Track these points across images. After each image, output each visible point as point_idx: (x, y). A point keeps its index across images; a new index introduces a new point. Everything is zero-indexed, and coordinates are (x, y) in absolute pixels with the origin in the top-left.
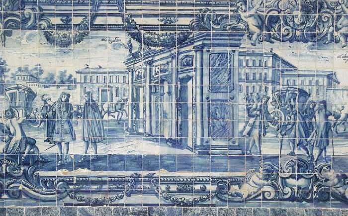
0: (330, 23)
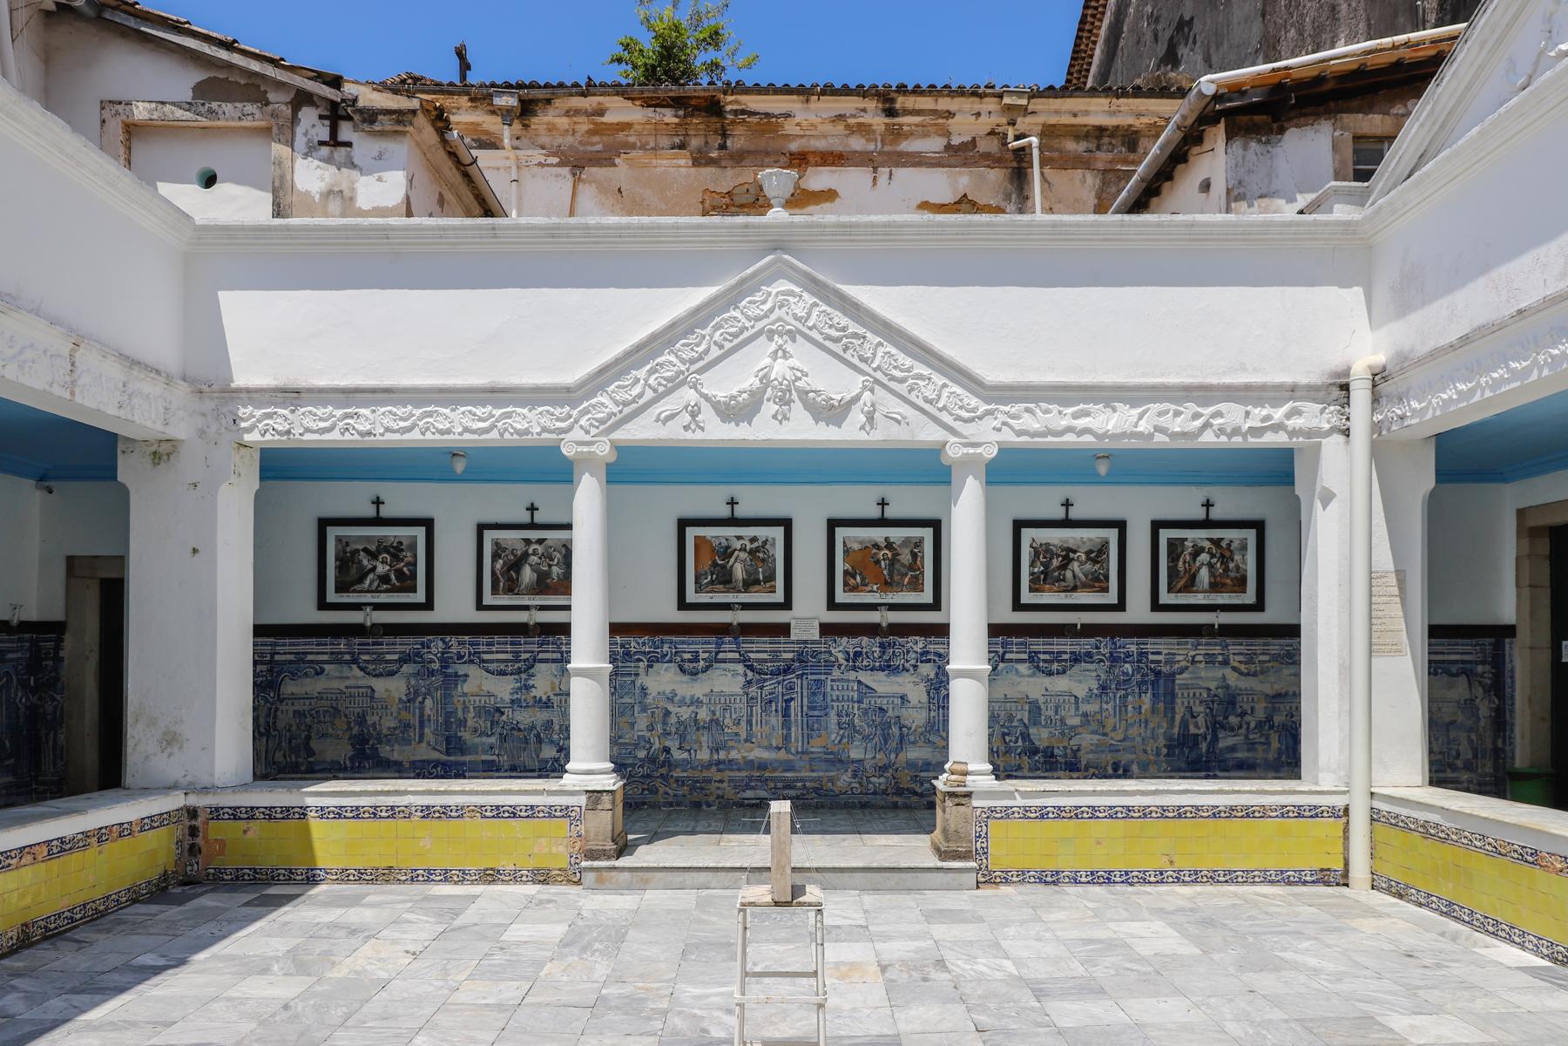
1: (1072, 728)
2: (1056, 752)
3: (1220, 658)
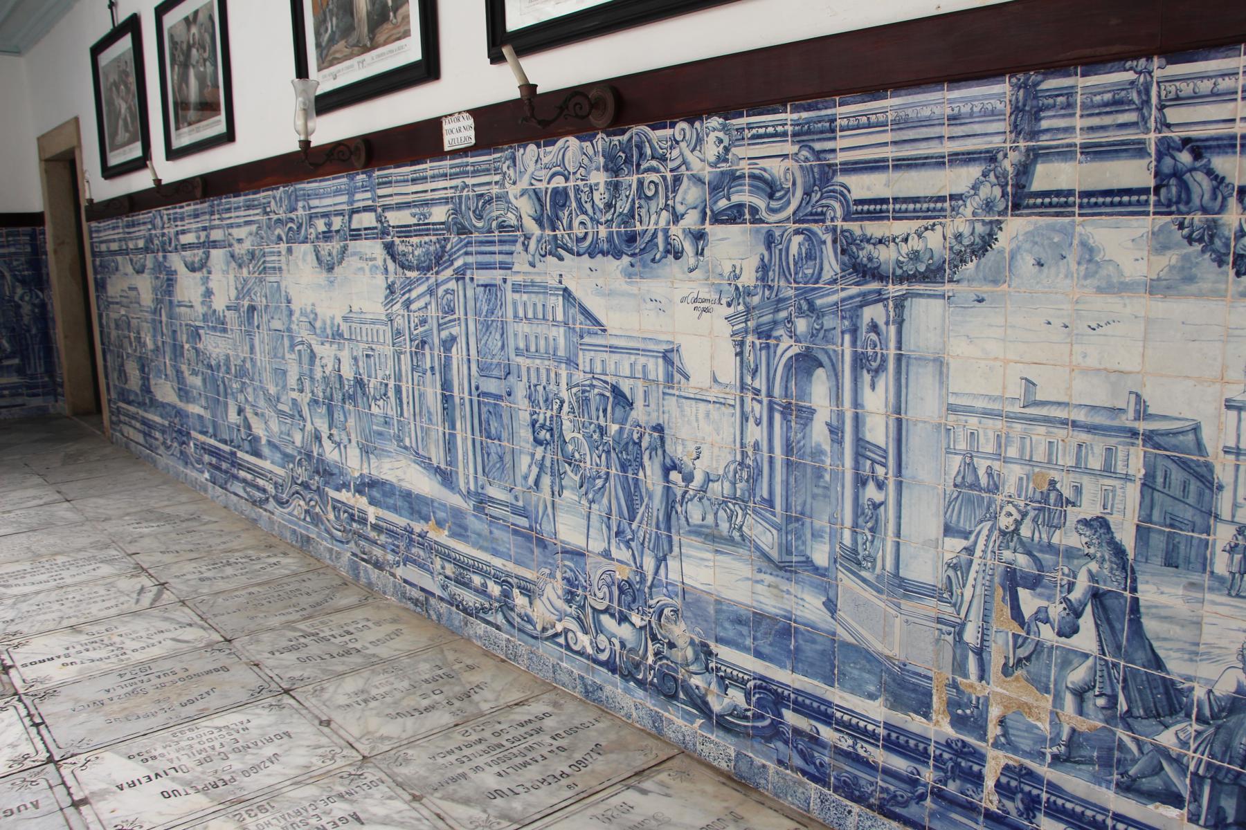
0: (662, 202)
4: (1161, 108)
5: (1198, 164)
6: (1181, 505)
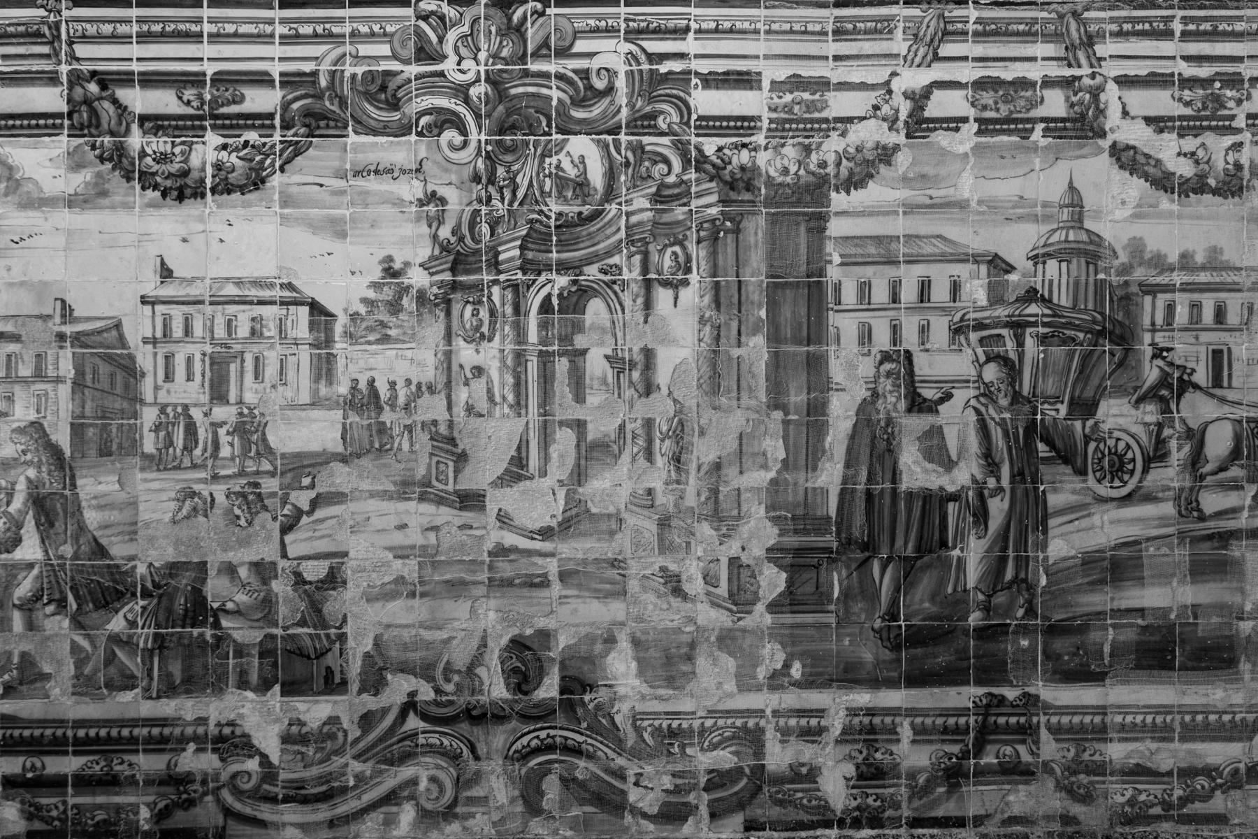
1: (302, 466)
2: (216, 588)
3: (1055, 104)
4: (70, 43)
5: (104, 94)
6: (111, 398)
